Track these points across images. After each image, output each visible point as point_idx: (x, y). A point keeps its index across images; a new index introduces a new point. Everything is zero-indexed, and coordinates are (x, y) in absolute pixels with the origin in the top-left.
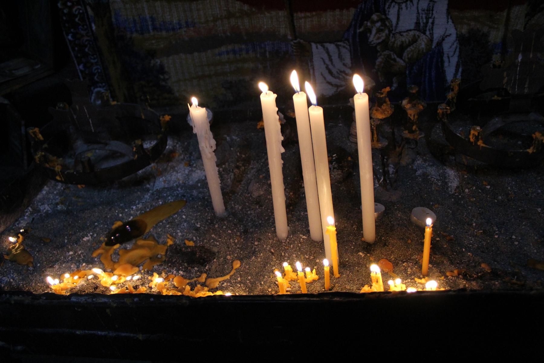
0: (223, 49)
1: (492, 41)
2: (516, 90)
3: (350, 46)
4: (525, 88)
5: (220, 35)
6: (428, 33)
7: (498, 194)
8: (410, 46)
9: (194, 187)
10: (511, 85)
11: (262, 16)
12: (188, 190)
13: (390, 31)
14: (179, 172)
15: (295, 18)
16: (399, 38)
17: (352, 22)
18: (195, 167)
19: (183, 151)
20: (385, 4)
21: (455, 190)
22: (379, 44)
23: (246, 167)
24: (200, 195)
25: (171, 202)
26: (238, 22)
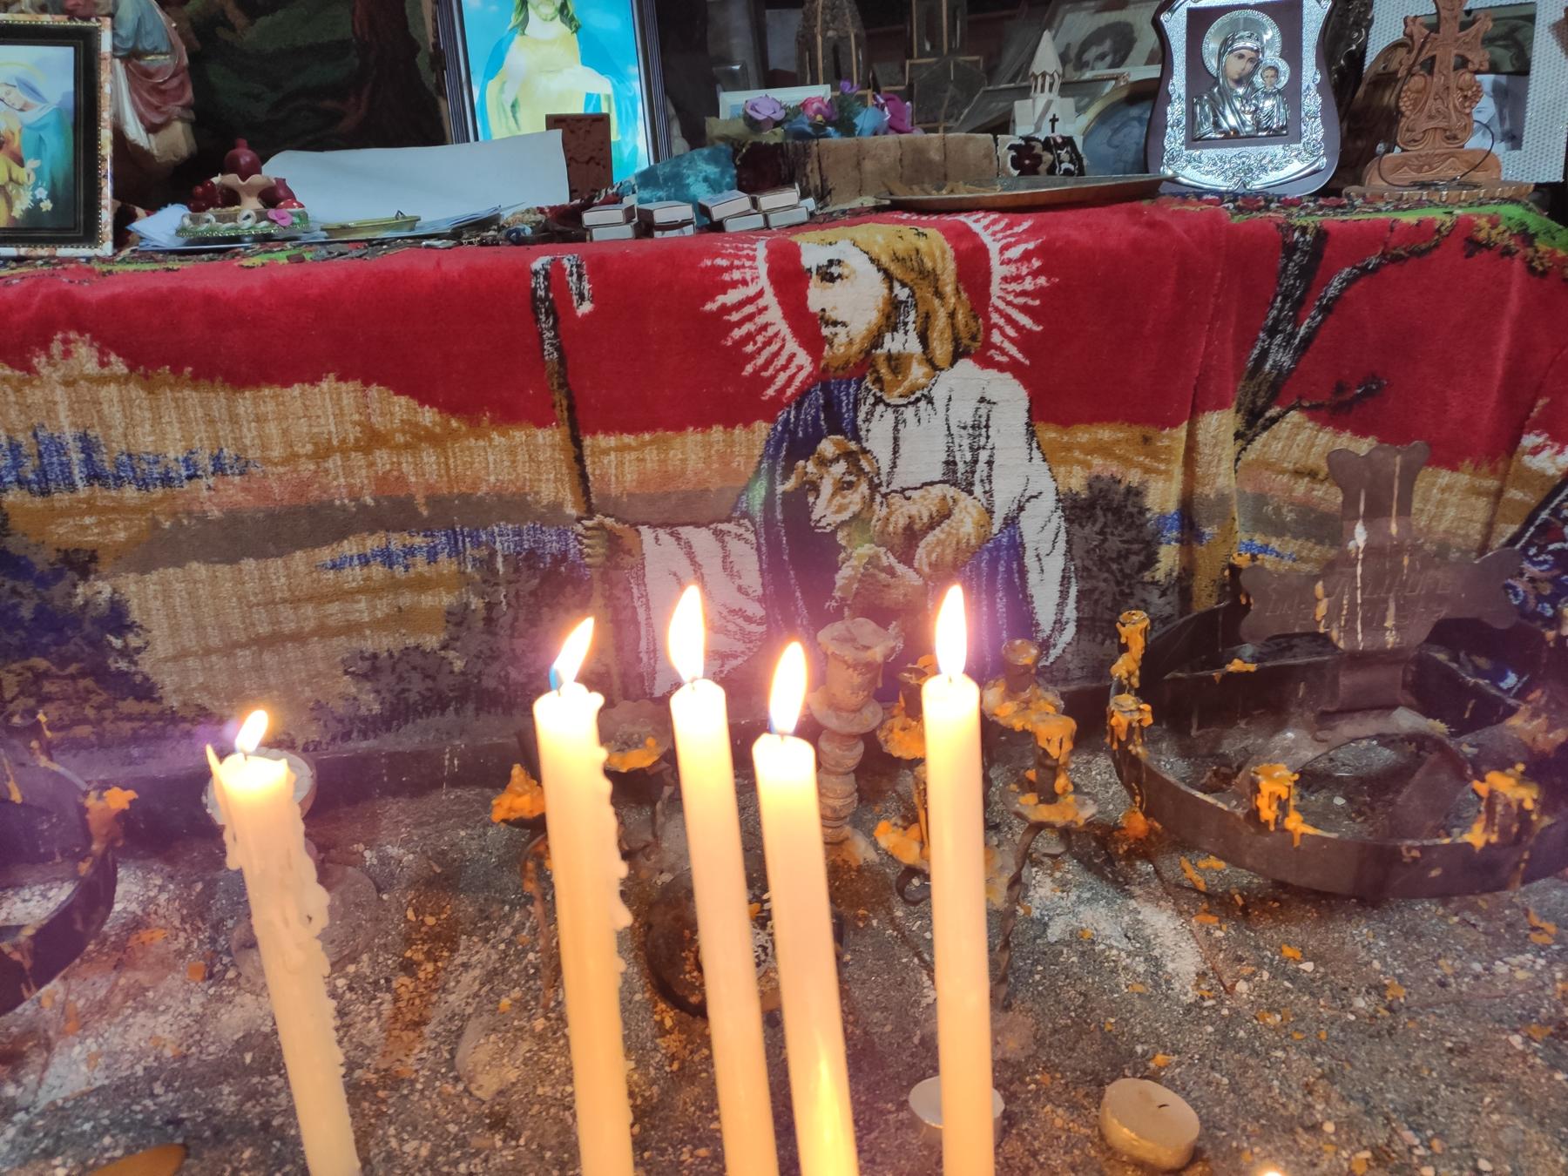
0: (349, 547)
1: (1156, 509)
2: (1360, 637)
3: (756, 533)
4: (1386, 629)
5: (337, 503)
6: (978, 490)
7: (1345, 989)
8: (933, 528)
9: (224, 1070)
10: (1343, 623)
11: (481, 443)
12: (196, 1090)
13: (874, 487)
14: (161, 1008)
15: (587, 452)
16: (901, 506)
17: (760, 463)
18: (231, 983)
19: (183, 921)
20: (856, 409)
21: (1197, 986)
22: (843, 524)
23: (440, 964)
24: (253, 1110)
25: (112, 1160)
26: (400, 464)
